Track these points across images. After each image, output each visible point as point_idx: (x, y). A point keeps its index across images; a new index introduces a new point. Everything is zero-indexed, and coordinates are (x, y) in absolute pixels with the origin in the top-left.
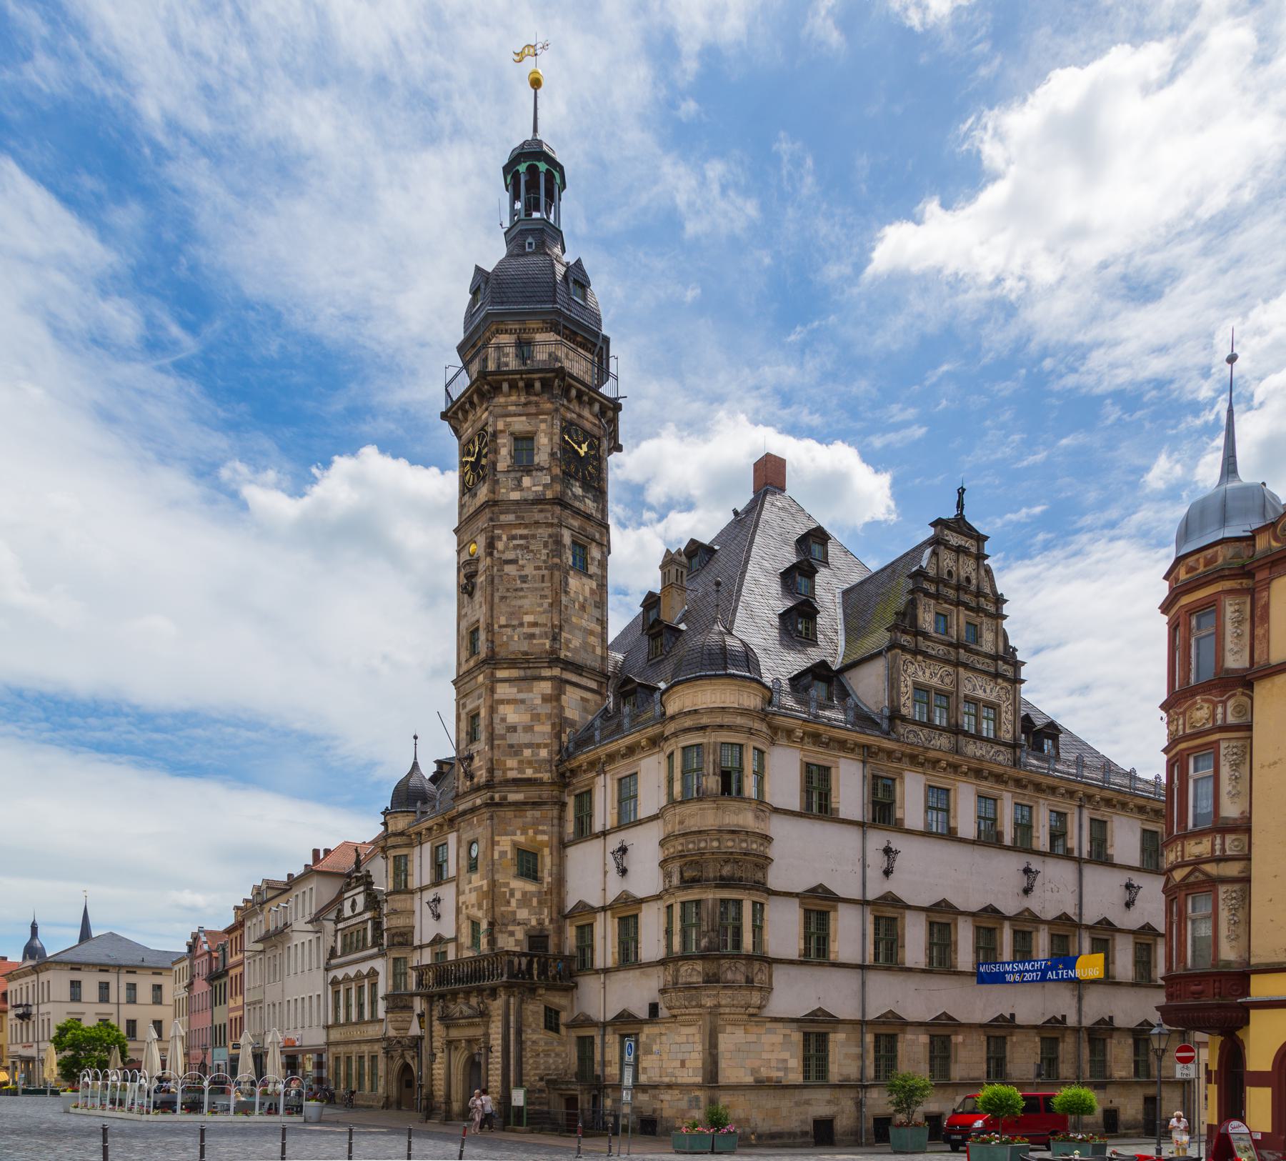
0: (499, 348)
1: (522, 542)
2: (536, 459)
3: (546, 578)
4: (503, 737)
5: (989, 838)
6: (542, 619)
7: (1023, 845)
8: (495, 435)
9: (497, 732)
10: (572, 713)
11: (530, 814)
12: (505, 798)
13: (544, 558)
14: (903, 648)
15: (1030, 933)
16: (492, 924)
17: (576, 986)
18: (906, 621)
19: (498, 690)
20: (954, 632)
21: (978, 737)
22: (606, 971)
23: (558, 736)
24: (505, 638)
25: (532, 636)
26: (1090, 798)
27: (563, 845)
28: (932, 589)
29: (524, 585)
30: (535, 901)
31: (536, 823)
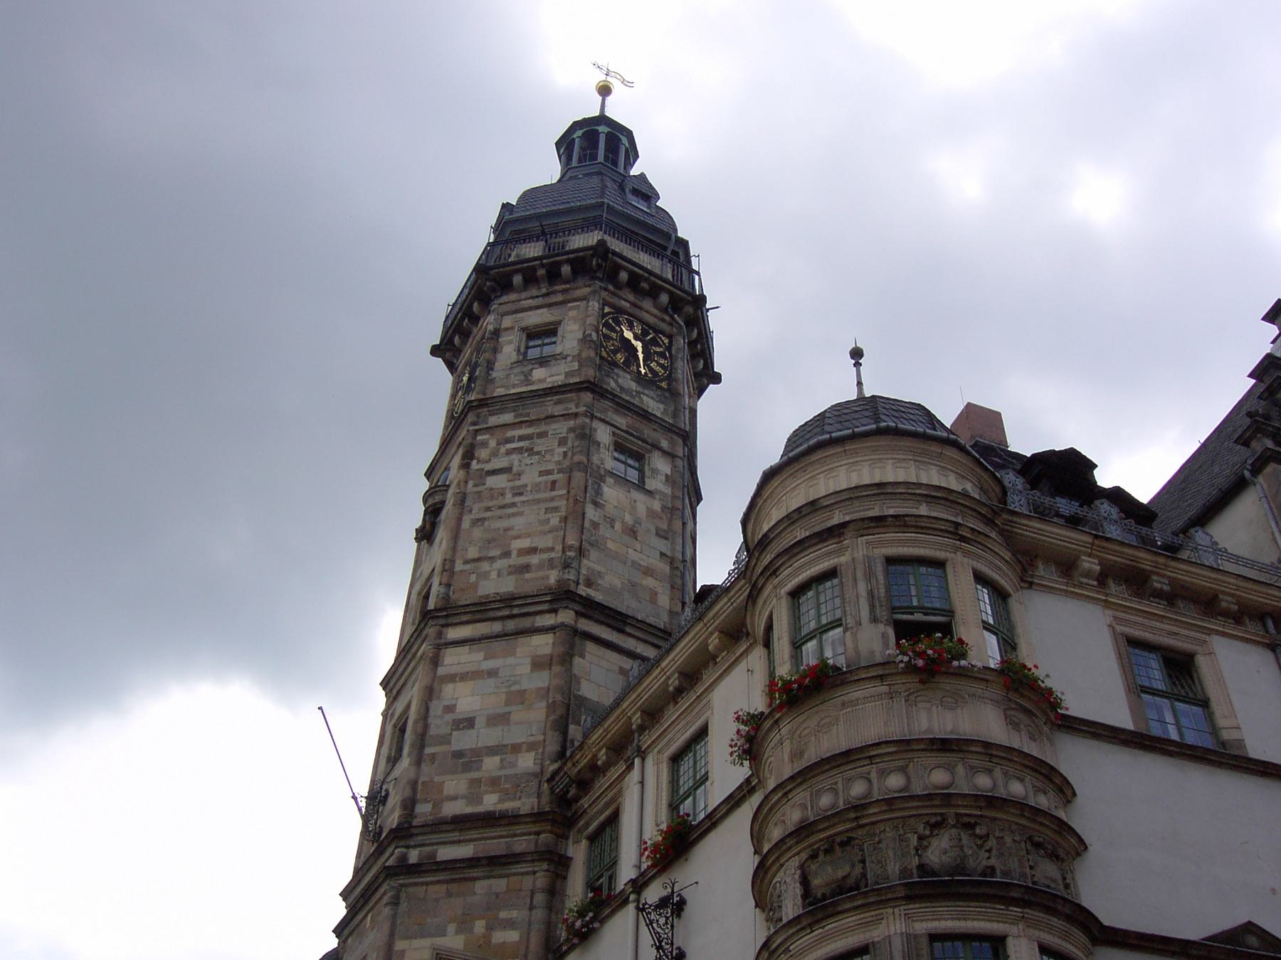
1: (521, 444)
4: (445, 740)
6: (546, 541)
9: (433, 731)
23: (562, 726)
25: (526, 568)
29: (517, 499)
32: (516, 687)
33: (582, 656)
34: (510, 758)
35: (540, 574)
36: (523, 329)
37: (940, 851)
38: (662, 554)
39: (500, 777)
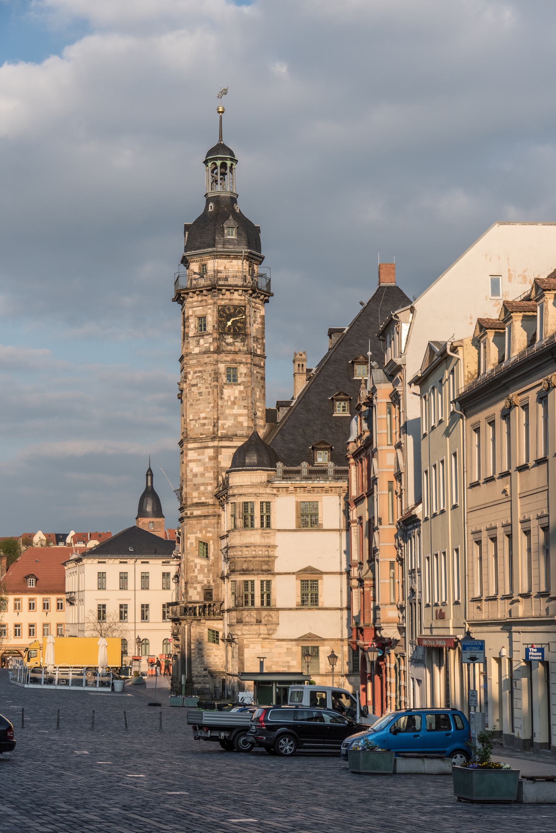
3: (211, 393)
4: (191, 480)
9: (188, 477)
11: (204, 522)
12: (192, 514)
13: (209, 382)
24: (192, 427)
25: (204, 424)
29: (201, 398)
30: (206, 569)
31: (206, 527)
34: (206, 487)
36: (196, 316)
38: (244, 406)
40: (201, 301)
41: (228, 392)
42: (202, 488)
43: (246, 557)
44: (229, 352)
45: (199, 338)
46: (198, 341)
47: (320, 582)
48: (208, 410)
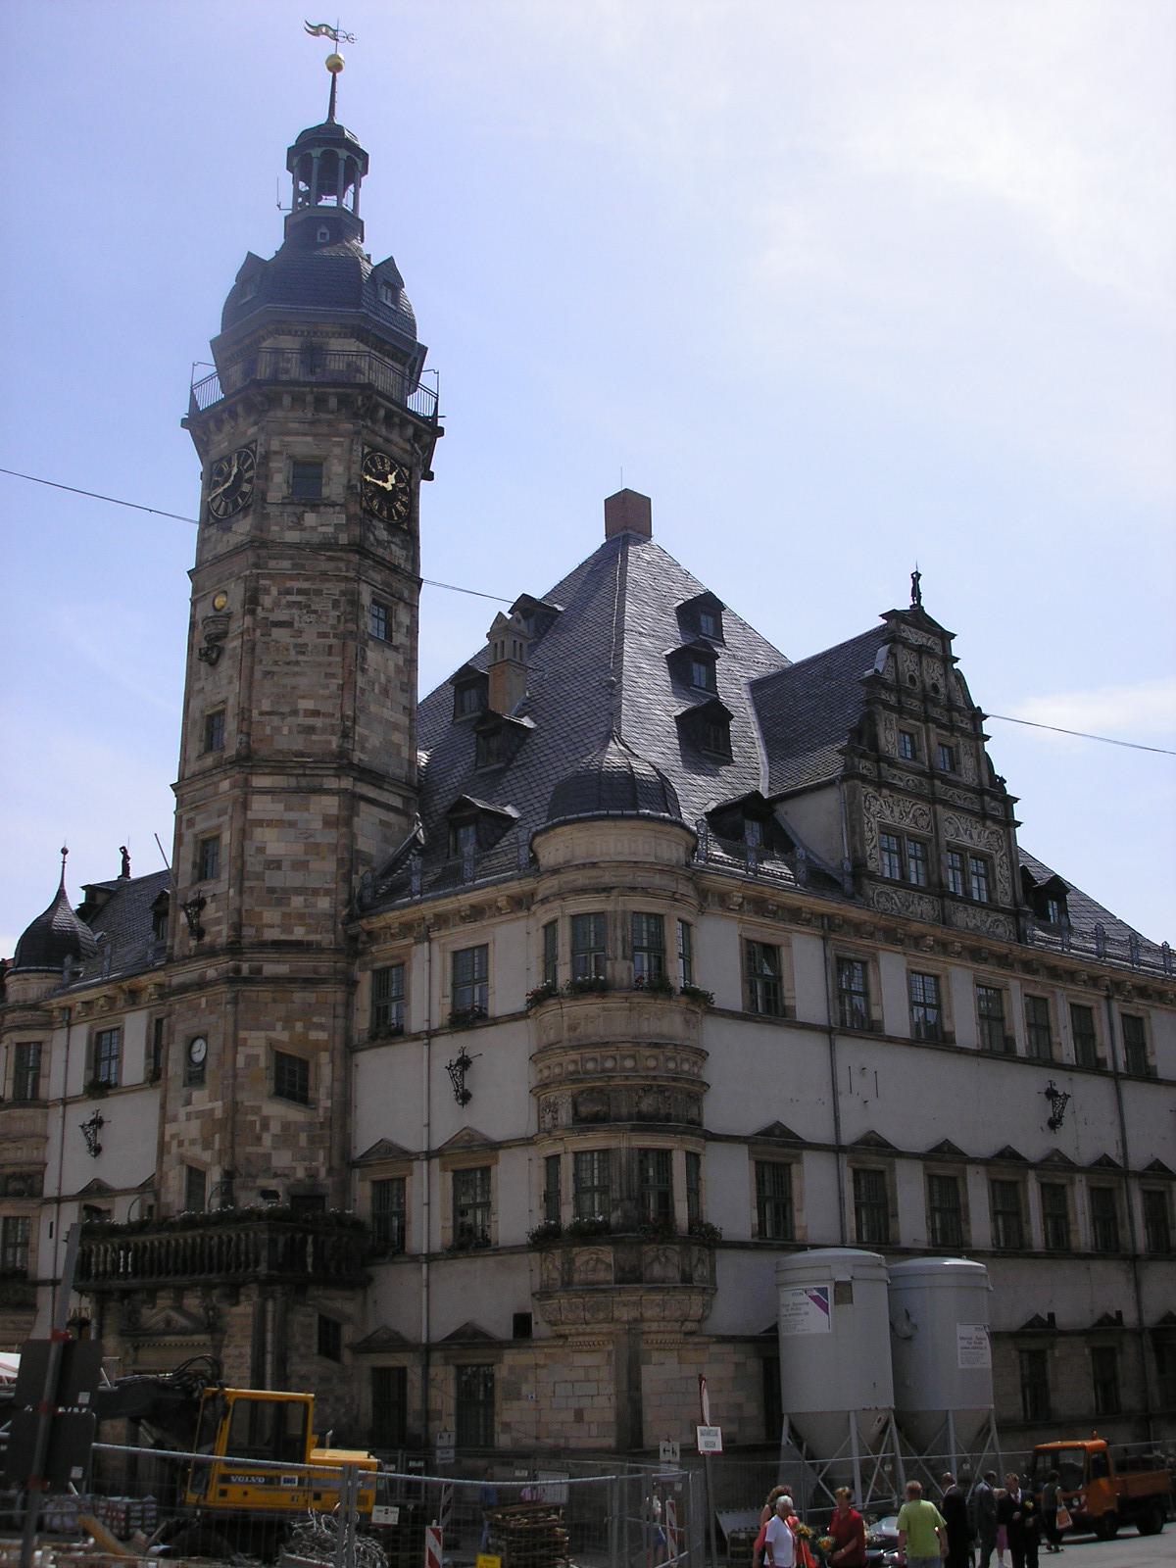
0: (277, 351)
1: (299, 598)
2: (326, 491)
4: (260, 877)
5: (997, 1049)
7: (1042, 1058)
8: (266, 457)
9: (249, 868)
10: (366, 844)
12: (259, 970)
14: (863, 779)
15: (1063, 1187)
16: (229, 1176)
17: (370, 1280)
18: (863, 740)
19: (255, 806)
20: (924, 755)
21: (967, 899)
22: (431, 1258)
23: (347, 878)
24: (268, 730)
25: (311, 730)
26: (1118, 986)
27: (351, 1048)
28: (893, 699)
29: (301, 658)
30: (303, 1138)
32: (312, 840)
33: (358, 816)
35: (323, 738)
36: (290, 457)
37: (647, 1105)
38: (405, 708)
39: (304, 914)
40: (313, 423)
41: (373, 655)
42: (297, 901)
43: (655, 1078)
44: (382, 563)
45: (302, 509)
46: (300, 518)
47: (794, 1168)
48: (327, 692)
